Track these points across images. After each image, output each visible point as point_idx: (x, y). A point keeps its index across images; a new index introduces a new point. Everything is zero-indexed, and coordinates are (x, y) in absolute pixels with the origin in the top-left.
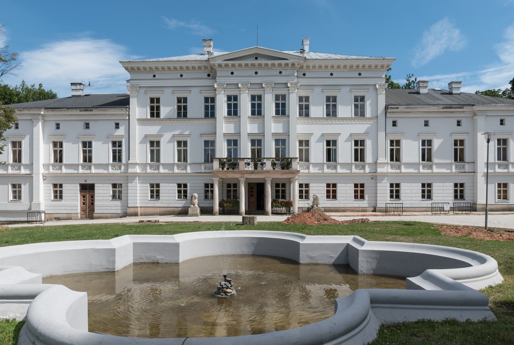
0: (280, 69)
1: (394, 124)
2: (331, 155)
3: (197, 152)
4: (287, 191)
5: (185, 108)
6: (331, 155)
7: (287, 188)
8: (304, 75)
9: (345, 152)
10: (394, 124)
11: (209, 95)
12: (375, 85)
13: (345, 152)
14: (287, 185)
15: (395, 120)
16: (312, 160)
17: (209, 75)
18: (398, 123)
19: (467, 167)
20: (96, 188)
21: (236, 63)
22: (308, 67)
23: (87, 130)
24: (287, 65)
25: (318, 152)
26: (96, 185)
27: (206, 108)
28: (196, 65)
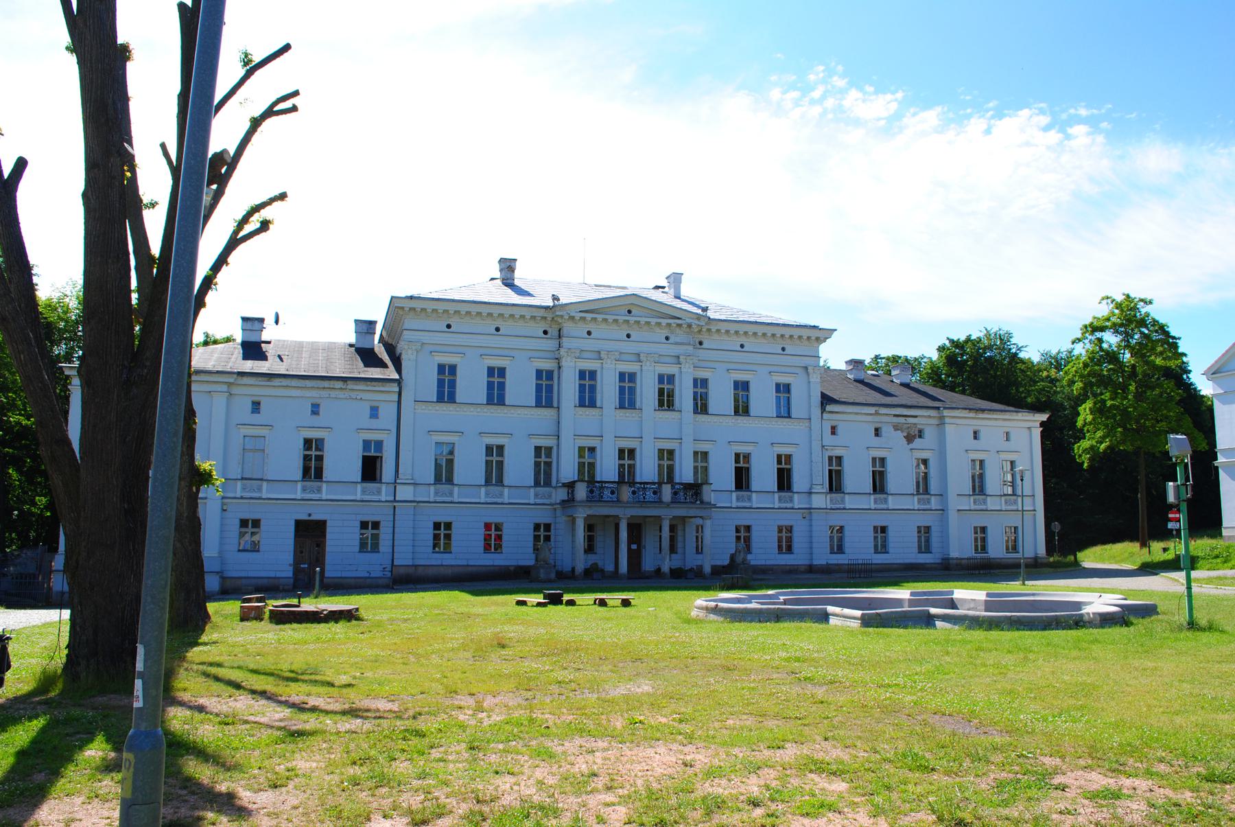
0: (666, 332)
1: (834, 431)
2: (742, 478)
3: (519, 467)
4: (680, 539)
5: (502, 386)
6: (742, 478)
7: (680, 533)
8: (701, 343)
9: (764, 475)
10: (834, 431)
11: (547, 365)
12: (806, 368)
13: (764, 475)
14: (680, 528)
15: (834, 423)
16: (989, 490)
17: (545, 332)
18: (839, 430)
19: (934, 503)
20: (328, 530)
21: (600, 317)
22: (709, 330)
23: (315, 417)
24: (679, 325)
25: (722, 475)
26: (328, 524)
27: (539, 388)
28: (528, 313)
